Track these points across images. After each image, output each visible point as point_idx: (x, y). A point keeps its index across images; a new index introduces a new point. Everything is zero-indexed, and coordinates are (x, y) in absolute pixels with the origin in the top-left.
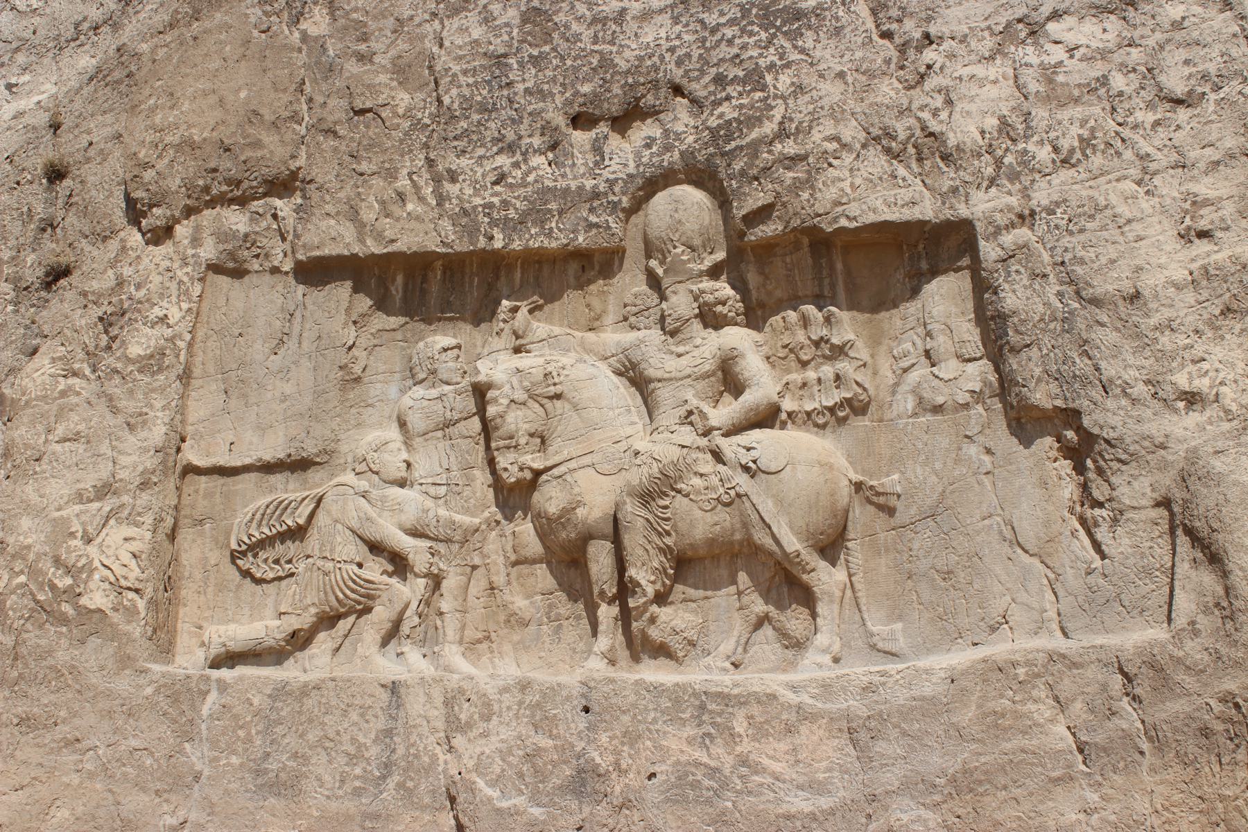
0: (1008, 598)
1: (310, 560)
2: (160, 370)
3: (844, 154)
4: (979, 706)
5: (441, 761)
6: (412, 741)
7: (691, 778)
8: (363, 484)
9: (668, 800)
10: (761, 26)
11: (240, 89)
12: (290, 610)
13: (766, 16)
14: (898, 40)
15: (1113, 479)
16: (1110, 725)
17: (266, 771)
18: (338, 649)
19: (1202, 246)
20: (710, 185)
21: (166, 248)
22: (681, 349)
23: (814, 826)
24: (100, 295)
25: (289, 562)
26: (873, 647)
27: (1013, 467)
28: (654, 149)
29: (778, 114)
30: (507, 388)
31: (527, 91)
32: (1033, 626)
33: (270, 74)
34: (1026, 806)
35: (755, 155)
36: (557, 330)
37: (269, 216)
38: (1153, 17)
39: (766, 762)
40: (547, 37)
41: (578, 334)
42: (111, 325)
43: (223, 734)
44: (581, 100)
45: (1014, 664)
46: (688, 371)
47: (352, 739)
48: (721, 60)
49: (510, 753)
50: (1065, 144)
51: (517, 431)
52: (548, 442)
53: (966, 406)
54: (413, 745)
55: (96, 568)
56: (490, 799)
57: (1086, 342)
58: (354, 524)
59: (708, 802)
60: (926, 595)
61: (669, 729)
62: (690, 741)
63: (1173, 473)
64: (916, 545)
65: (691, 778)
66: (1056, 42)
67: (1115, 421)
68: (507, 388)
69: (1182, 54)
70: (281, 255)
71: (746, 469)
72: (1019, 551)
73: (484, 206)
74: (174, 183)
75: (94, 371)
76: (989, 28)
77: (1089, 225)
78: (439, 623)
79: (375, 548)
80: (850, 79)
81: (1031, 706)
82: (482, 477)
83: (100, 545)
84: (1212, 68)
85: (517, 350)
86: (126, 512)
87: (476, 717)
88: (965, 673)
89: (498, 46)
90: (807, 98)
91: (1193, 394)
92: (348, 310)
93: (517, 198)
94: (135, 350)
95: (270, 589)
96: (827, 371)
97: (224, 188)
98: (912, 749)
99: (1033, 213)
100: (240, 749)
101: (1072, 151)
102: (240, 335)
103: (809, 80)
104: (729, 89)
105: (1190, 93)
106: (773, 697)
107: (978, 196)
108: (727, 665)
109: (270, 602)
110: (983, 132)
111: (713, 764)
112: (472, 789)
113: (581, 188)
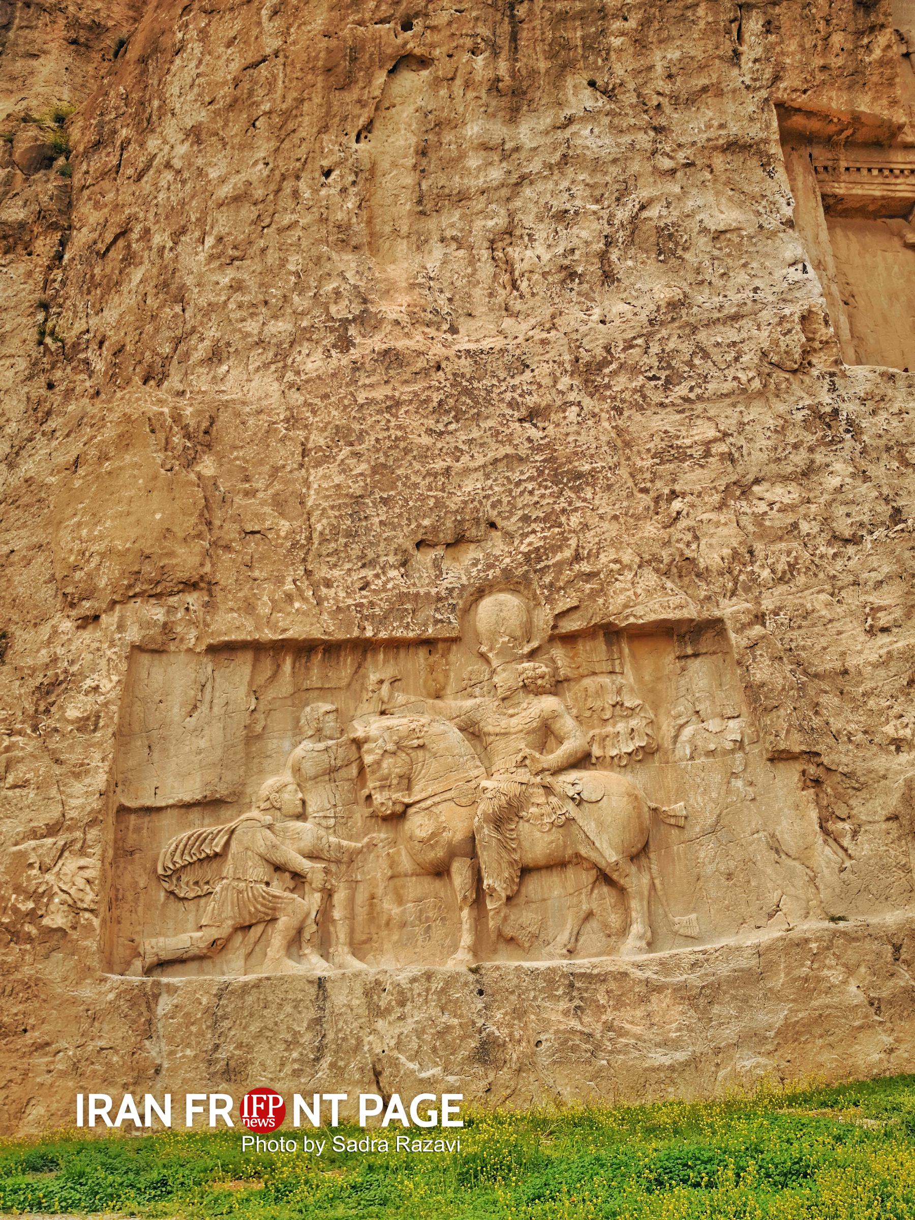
0: (779, 891)
1: (225, 881)
2: (94, 731)
3: (626, 572)
4: (787, 974)
5: (365, 1042)
6: (340, 1027)
7: (570, 1043)
8: (268, 819)
9: (554, 1062)
10: (552, 482)
11: (154, 513)
12: (211, 923)
13: (556, 475)
14: (652, 494)
15: (851, 802)
16: (891, 984)
17: (217, 1060)
18: (249, 955)
19: (884, 639)
20: (526, 592)
21: (98, 634)
22: (511, 711)
23: (675, 1075)
24: (34, 670)
25: (207, 883)
26: (676, 933)
27: (772, 795)
28: (480, 567)
29: (573, 542)
30: (381, 740)
31: (381, 522)
32: (803, 912)
33: (177, 502)
34: (839, 1050)
35: (560, 572)
36: (413, 699)
37: (182, 610)
38: (821, 484)
39: (628, 1026)
40: (393, 486)
41: (431, 701)
42: (48, 693)
43: (177, 1030)
44: (423, 531)
45: (807, 941)
46: (520, 727)
47: (288, 1028)
48: (527, 505)
49: (423, 1031)
50: (781, 567)
51: (390, 774)
52: (414, 783)
53: (733, 751)
54: (340, 1030)
55: (56, 893)
56: (413, 1072)
57: (817, 704)
58: (262, 850)
59: (588, 1062)
60: (713, 893)
61: (547, 1004)
62: (566, 1013)
63: (897, 795)
64: (702, 854)
65: (570, 1043)
66: (760, 499)
67: (845, 760)
68: (381, 740)
69: (842, 510)
70: (193, 641)
71: (573, 799)
72: (783, 856)
73: (356, 605)
74: (102, 582)
75: (35, 729)
76: (715, 488)
77: (804, 623)
78: (332, 929)
79: (278, 868)
80: (622, 520)
81: (826, 972)
82: (360, 812)
83: (58, 873)
84: (866, 519)
85: (383, 713)
86: (78, 846)
87: (394, 1003)
88: (769, 949)
89: (356, 488)
90: (592, 533)
91: (901, 740)
92: (250, 684)
93: (381, 600)
94: (72, 713)
95: (191, 905)
96: (621, 727)
97: (145, 587)
98: (741, 1010)
99: (764, 615)
100: (194, 1043)
101: (784, 572)
102: (161, 701)
103: (593, 521)
104: (534, 525)
105: (854, 535)
106: (625, 974)
107: (724, 602)
108: (565, 951)
109: (191, 917)
110: (723, 559)
111: (586, 1030)
112: (395, 1064)
113: (428, 594)
